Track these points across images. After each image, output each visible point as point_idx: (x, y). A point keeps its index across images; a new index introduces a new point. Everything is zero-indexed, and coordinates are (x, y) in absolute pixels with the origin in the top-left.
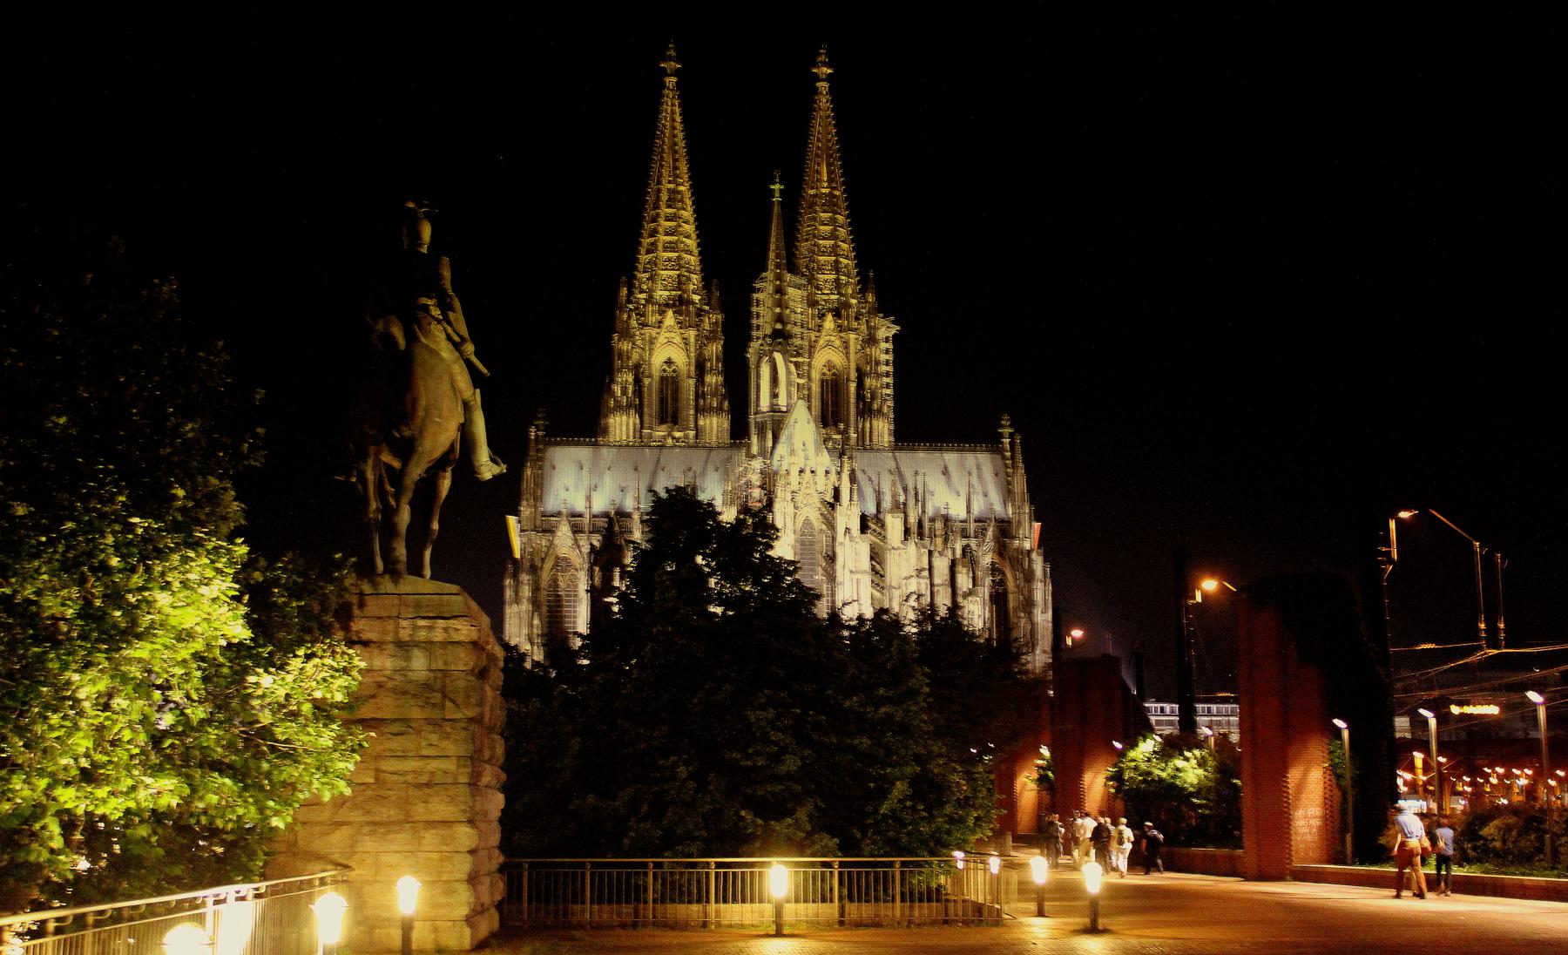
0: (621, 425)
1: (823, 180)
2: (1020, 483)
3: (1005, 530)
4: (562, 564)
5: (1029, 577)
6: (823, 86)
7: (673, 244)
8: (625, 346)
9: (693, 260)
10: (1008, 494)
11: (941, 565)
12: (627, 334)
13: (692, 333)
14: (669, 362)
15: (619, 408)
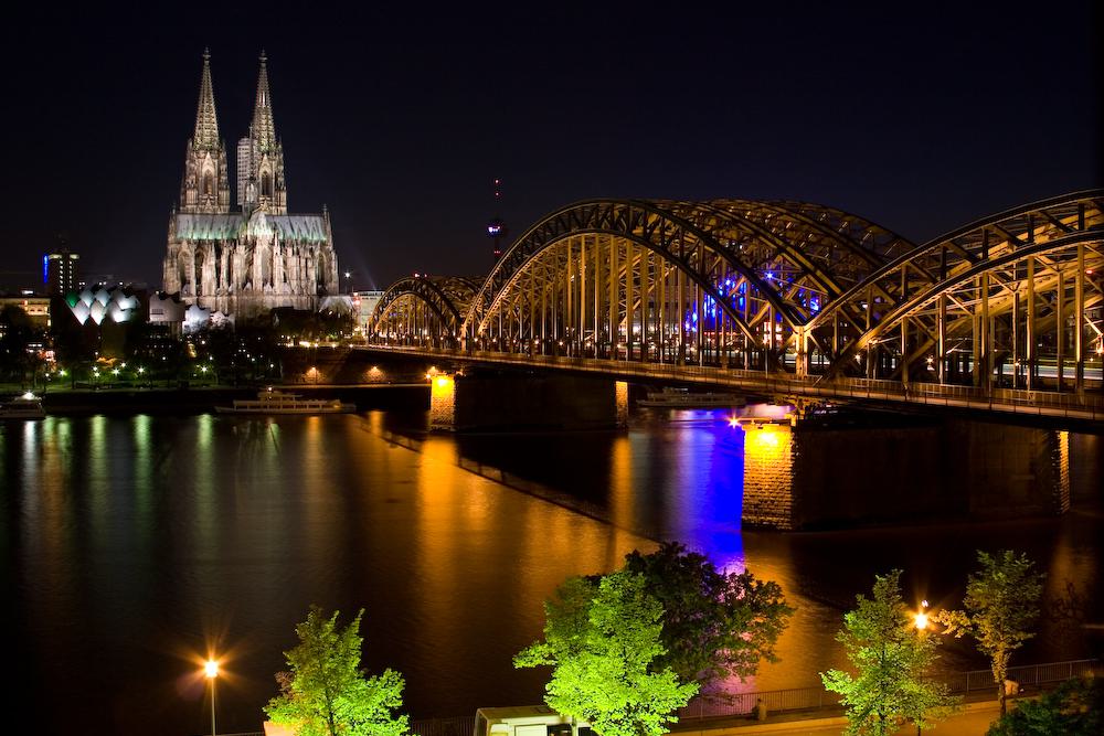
0: (191, 194)
1: (263, 100)
2: (329, 228)
3: (323, 244)
4: (185, 254)
5: (331, 260)
6: (264, 65)
7: (208, 126)
8: (193, 165)
9: (216, 132)
10: (325, 233)
11: (303, 261)
12: (193, 161)
13: (216, 161)
14: (208, 171)
15: (190, 188)
